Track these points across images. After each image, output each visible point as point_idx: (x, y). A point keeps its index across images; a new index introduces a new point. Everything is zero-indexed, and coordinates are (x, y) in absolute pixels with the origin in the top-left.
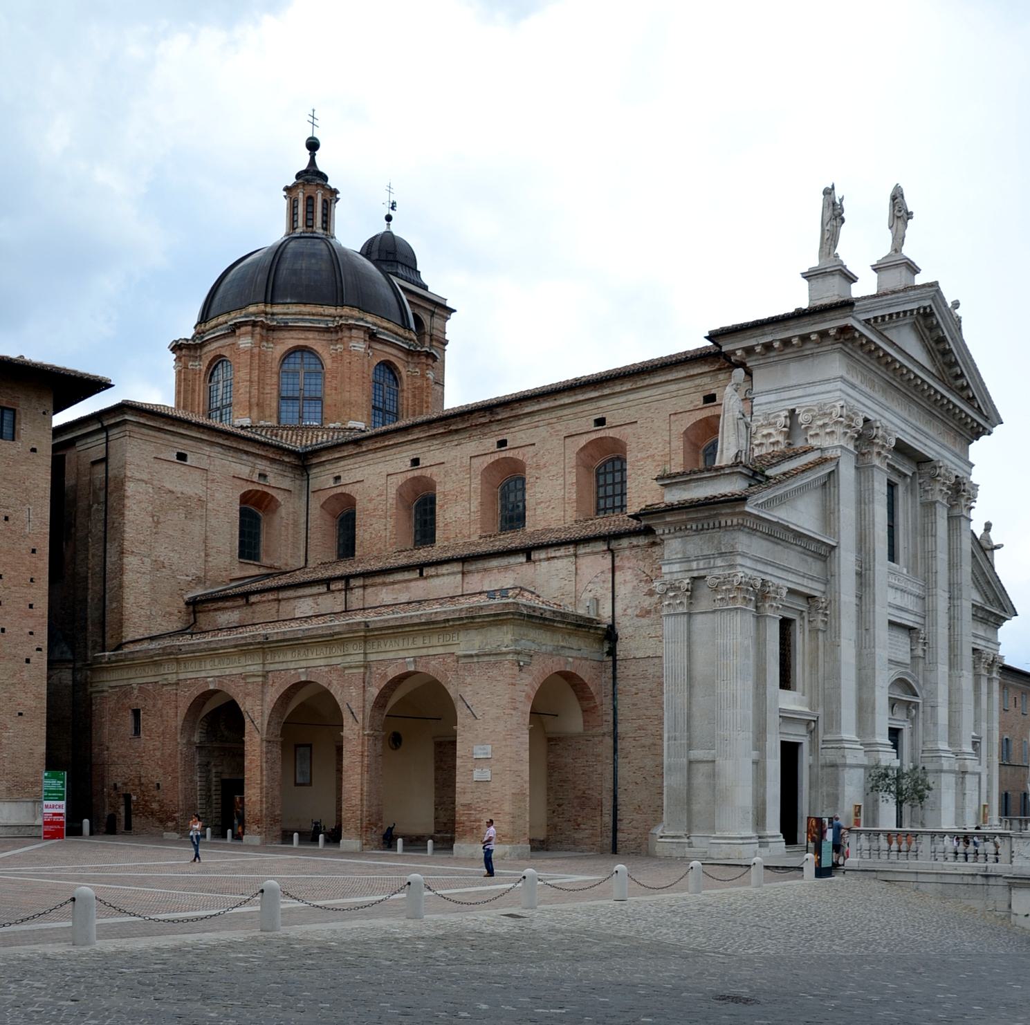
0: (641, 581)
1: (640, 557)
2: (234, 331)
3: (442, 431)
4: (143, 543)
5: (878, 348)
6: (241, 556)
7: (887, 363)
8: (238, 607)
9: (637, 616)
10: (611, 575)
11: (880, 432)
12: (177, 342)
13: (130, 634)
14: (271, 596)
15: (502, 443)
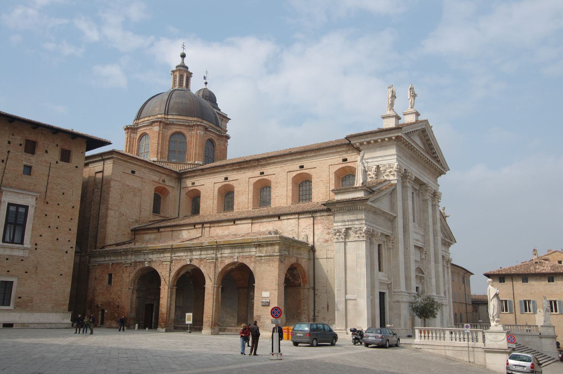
0: (324, 229)
2: (152, 124)
3: (238, 167)
4: (116, 205)
5: (409, 143)
6: (153, 212)
7: (411, 148)
8: (154, 233)
9: (323, 242)
10: (313, 226)
11: (410, 174)
12: (127, 126)
13: (109, 242)
14: (169, 229)
15: (262, 173)
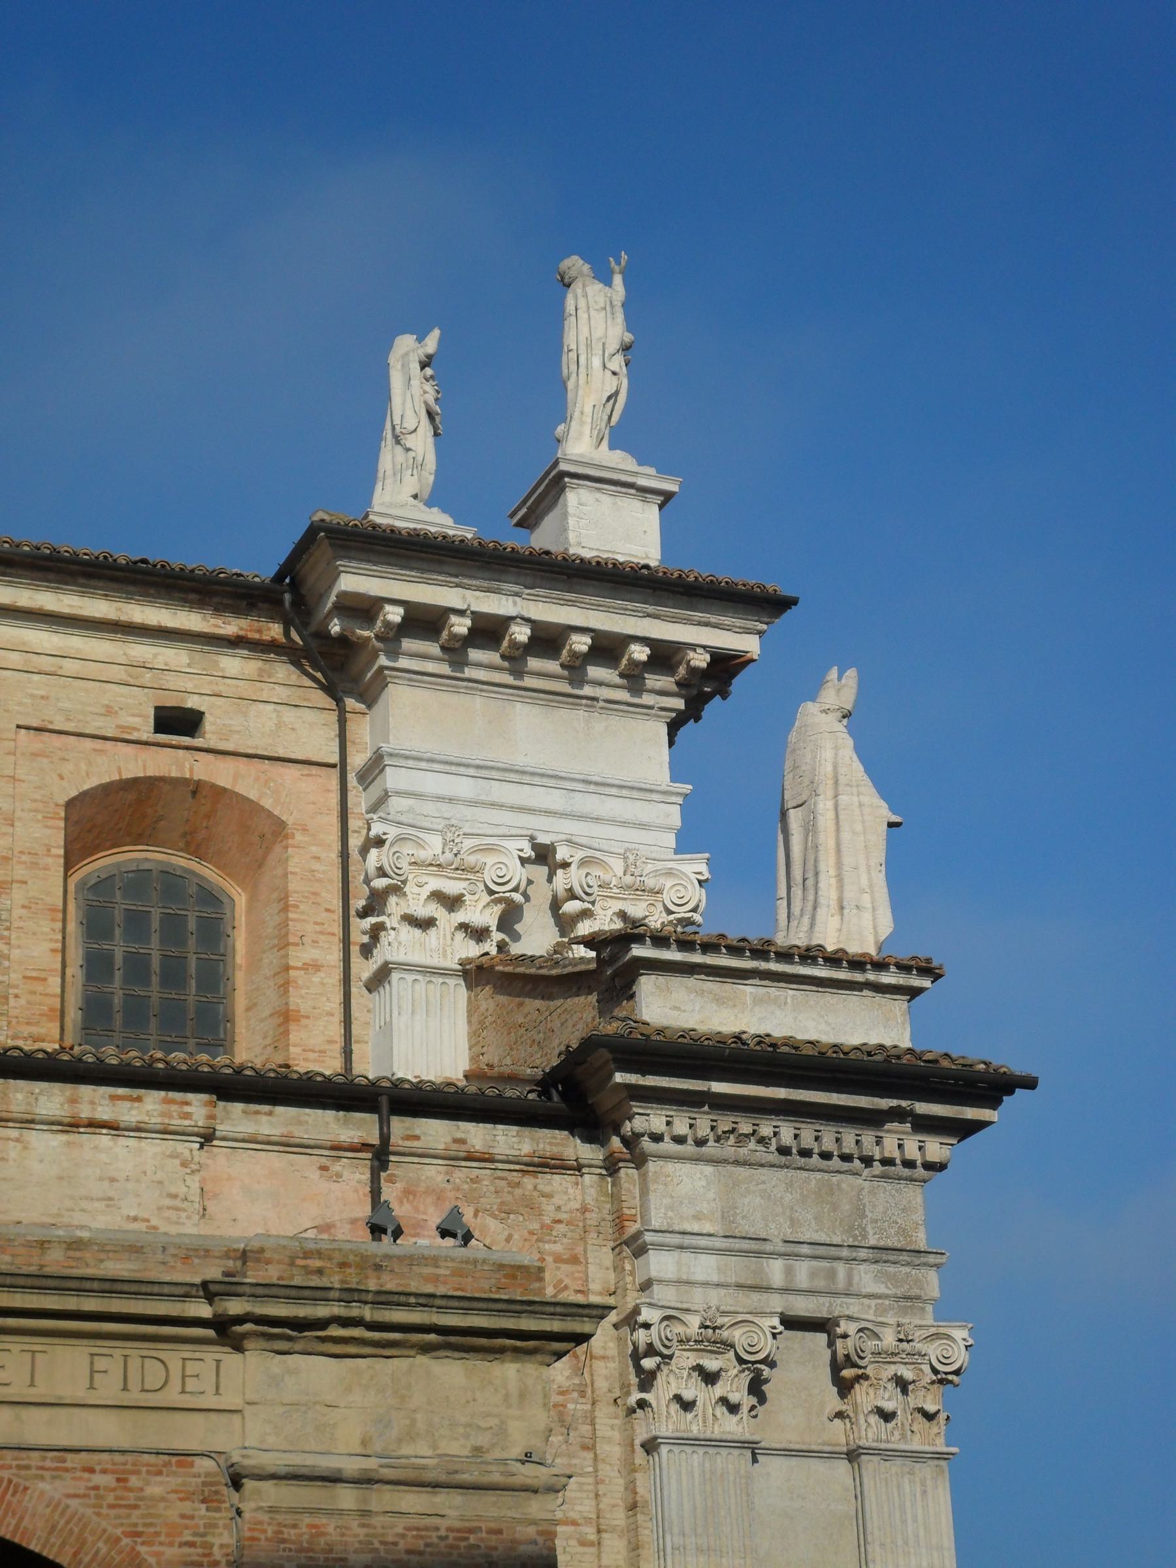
1: (490, 1201)
